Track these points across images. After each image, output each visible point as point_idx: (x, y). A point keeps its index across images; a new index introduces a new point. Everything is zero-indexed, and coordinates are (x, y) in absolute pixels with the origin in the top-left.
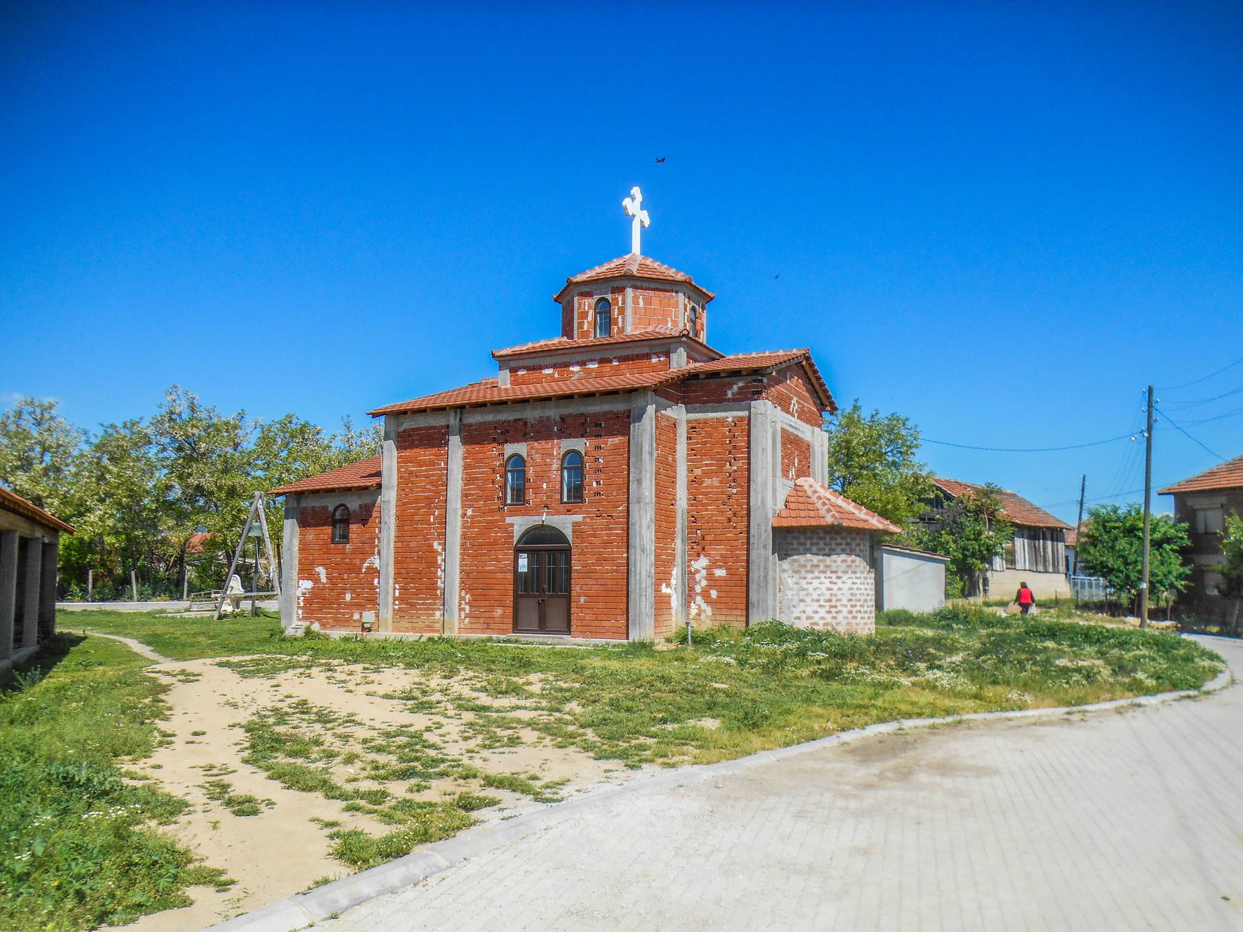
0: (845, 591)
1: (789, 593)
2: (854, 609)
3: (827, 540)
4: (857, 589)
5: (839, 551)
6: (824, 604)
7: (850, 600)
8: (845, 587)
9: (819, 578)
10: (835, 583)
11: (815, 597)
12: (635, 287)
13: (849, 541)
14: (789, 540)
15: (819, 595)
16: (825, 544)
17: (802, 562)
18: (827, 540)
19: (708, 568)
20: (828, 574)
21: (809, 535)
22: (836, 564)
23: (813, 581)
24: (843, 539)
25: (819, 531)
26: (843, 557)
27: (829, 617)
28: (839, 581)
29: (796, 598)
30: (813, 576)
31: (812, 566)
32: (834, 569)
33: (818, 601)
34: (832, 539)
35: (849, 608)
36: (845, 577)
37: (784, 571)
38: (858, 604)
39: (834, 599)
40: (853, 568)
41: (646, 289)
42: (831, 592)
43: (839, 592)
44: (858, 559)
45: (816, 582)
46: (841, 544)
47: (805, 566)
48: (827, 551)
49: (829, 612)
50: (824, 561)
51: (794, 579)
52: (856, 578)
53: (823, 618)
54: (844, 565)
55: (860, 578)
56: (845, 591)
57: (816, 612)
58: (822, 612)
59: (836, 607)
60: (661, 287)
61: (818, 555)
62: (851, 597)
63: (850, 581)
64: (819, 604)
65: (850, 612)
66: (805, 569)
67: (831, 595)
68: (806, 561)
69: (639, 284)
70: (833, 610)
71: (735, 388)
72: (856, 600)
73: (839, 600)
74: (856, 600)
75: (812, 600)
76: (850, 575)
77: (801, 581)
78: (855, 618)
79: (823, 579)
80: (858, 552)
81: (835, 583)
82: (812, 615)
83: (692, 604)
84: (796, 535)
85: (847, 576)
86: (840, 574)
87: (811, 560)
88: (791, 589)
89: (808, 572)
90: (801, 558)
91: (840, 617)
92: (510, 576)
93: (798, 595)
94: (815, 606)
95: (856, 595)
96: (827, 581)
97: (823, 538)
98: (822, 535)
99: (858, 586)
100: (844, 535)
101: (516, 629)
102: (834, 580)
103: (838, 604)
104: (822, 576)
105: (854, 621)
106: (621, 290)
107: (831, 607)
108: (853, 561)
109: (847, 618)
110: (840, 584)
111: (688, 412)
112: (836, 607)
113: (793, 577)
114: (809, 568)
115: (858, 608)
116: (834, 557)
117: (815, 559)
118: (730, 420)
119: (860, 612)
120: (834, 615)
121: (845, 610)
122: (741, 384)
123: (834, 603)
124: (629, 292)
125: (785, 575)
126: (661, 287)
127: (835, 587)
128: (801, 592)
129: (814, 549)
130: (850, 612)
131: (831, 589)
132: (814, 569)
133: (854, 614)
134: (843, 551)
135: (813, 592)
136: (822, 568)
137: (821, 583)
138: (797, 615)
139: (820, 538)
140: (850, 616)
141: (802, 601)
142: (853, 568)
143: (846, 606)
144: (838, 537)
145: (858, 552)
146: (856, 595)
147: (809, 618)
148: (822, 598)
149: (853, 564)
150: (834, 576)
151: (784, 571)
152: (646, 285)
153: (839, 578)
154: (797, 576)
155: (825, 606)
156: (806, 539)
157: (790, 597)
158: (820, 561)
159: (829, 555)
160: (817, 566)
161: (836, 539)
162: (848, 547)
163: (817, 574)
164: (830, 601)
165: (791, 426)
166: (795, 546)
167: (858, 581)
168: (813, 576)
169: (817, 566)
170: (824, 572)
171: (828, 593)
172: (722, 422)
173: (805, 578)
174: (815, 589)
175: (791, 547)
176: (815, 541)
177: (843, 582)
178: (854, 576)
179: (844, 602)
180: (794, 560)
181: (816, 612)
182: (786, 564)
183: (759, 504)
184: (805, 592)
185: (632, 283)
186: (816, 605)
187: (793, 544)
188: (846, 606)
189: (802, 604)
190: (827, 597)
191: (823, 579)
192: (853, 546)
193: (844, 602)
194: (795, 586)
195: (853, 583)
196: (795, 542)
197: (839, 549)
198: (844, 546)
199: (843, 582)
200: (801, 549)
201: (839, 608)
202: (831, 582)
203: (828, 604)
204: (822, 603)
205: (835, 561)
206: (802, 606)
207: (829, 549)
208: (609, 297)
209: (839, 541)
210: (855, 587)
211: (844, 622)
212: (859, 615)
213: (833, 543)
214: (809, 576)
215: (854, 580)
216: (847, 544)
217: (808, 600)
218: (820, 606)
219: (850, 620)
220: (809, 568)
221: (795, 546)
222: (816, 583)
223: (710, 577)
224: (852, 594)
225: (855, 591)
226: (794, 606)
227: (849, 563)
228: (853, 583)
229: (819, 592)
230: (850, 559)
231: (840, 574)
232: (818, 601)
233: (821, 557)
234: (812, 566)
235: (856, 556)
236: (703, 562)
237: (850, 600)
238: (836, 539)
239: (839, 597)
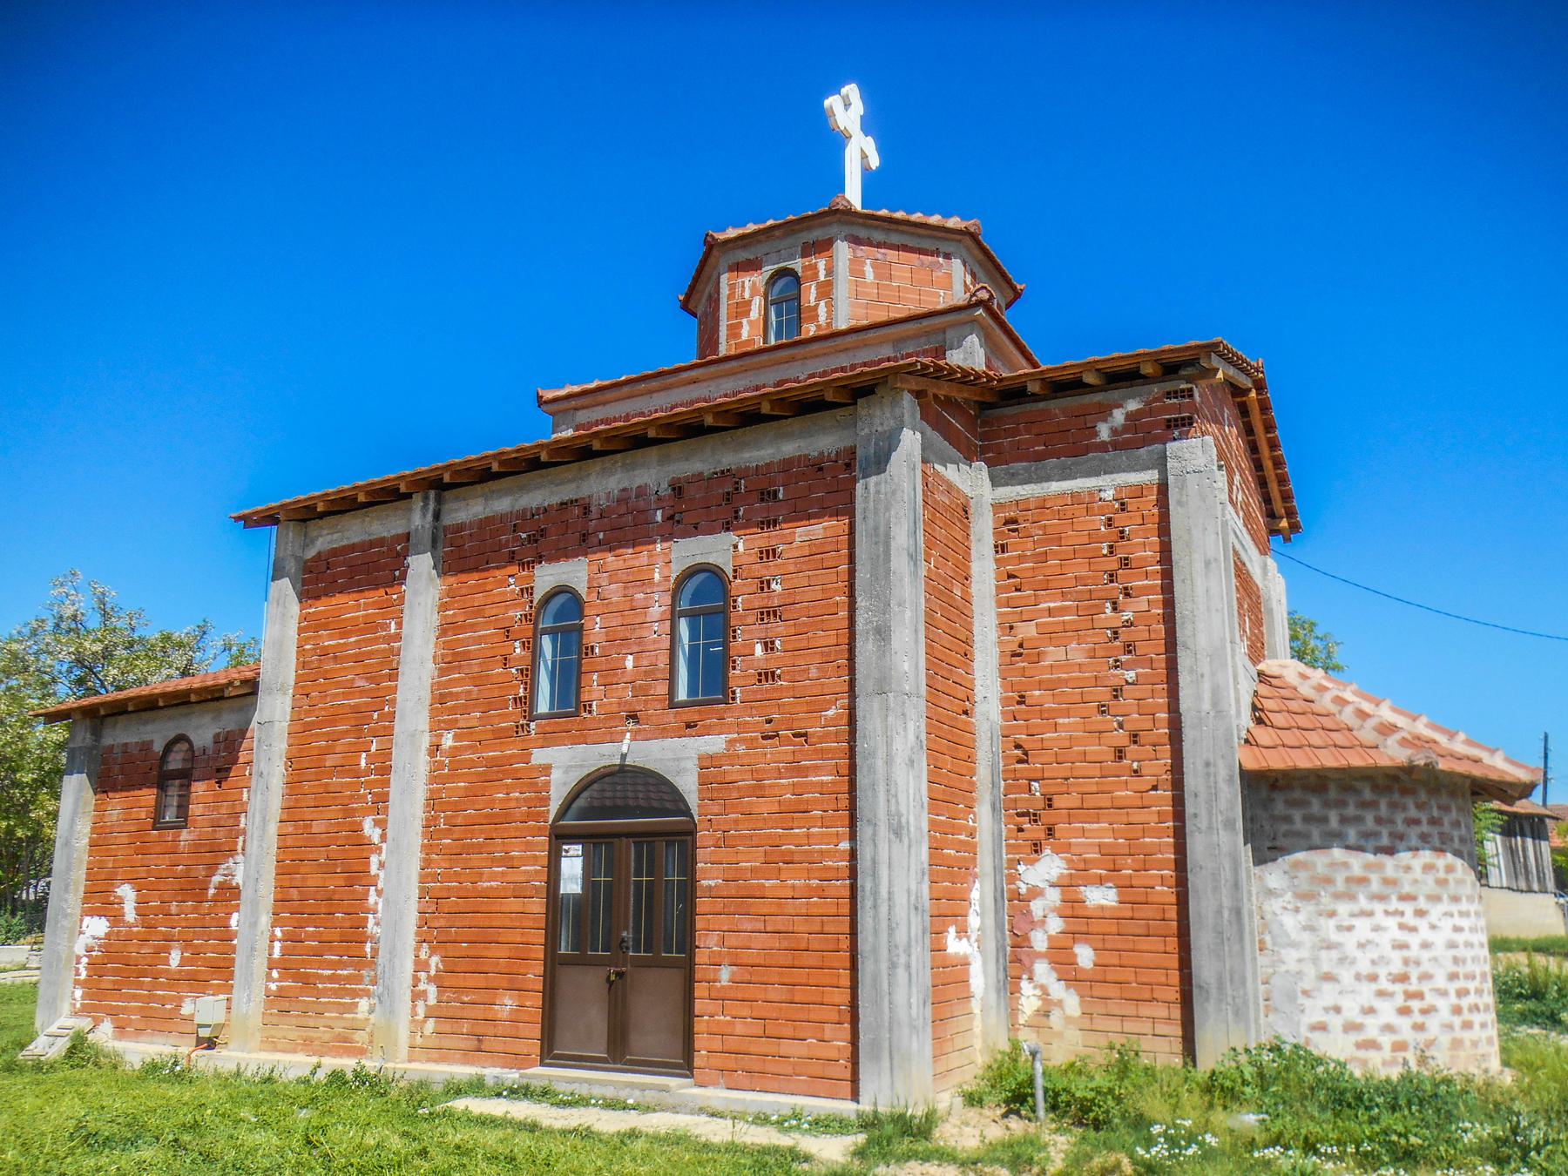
0: (1440, 950)
1: (1290, 956)
2: (1465, 1002)
3: (1384, 810)
6: (1390, 987)
7: (1453, 977)
8: (1439, 938)
9: (1370, 914)
10: (1413, 929)
11: (1364, 967)
12: (856, 241)
13: (1435, 813)
14: (1280, 808)
15: (1373, 962)
16: (1379, 821)
17: (1321, 869)
18: (1384, 810)
19: (1066, 885)
20: (1394, 904)
21: (1333, 794)
23: (1356, 922)
24: (1420, 806)
25: (1358, 785)
26: (1426, 856)
27: (1404, 1023)
28: (1422, 924)
29: (1310, 971)
30: (1355, 908)
31: (1349, 880)
32: (1407, 889)
33: (1373, 978)
34: (1393, 806)
35: (1453, 999)
36: (1436, 911)
37: (1271, 893)
39: (1414, 974)
41: (879, 246)
42: (1405, 953)
43: (1425, 955)
45: (1362, 925)
46: (1417, 822)
47: (1328, 881)
48: (1385, 841)
49: (1404, 1011)
50: (1380, 867)
51: (1302, 917)
52: (1461, 914)
53: (1388, 1028)
54: (1430, 879)
56: (1440, 950)
57: (1370, 1011)
58: (1387, 1011)
59: (1419, 995)
60: (911, 243)
61: (1361, 849)
62: (1454, 969)
64: (1374, 987)
66: (1331, 889)
67: (1406, 962)
68: (1332, 865)
70: (1415, 1005)
71: (1119, 416)
73: (1426, 977)
75: (1358, 977)
76: (1444, 906)
77: (1323, 921)
78: (1467, 1025)
79: (1380, 918)
81: (1413, 929)
82: (1359, 1019)
83: (1025, 985)
84: (1297, 794)
86: (1422, 903)
87: (1346, 865)
88: (1295, 945)
89: (1338, 896)
90: (1319, 860)
91: (1433, 1024)
92: (538, 906)
93: (1315, 961)
94: (1366, 992)
96: (1392, 923)
97: (1372, 805)
98: (1368, 795)
101: (550, 1052)
102: (1410, 919)
103: (1425, 987)
104: (1378, 907)
106: (824, 246)
107: (1409, 995)
109: (1450, 1027)
110: (1425, 933)
111: (995, 482)
112: (1419, 995)
113: (1297, 910)
114: (1340, 885)
116: (1404, 857)
117: (1358, 862)
118: (1109, 495)
120: (1417, 1018)
121: (1444, 1005)
122: (1133, 405)
123: (1414, 986)
124: (843, 250)
125: (1274, 905)
126: (911, 243)
127: (1414, 940)
128: (1324, 954)
129: (1352, 834)
131: (1403, 946)
132: (1355, 888)
133: (1466, 1016)
134: (1424, 838)
135: (1358, 954)
136: (1375, 886)
137: (1376, 929)
138: (1319, 1017)
139: (1364, 805)
140: (1457, 1021)
141: (1328, 977)
143: (1444, 993)
144: (1410, 802)
146: (1464, 961)
147: (1351, 1027)
148: (1382, 972)
149: (1450, 877)
150: (1408, 908)
151: (1271, 893)
152: (878, 236)
153: (1420, 913)
154: (1308, 909)
155: (1391, 995)
156: (1327, 805)
157: (1292, 966)
158: (1368, 867)
159: (1390, 851)
160: (1363, 881)
161: (1404, 808)
162: (1435, 831)
163: (1363, 903)
164: (1403, 978)
166: (1299, 825)
168: (1355, 908)
169: (1363, 881)
170: (1381, 898)
171: (1396, 957)
172: (1087, 502)
173: (1332, 914)
174: (1361, 946)
175: (1284, 827)
176: (1351, 811)
178: (1454, 908)
179: (1440, 981)
180: (1297, 865)
181: (1370, 1011)
182: (1274, 875)
183: (1206, 706)
184: (1334, 954)
185: (846, 230)
186: (1367, 989)
187: (1288, 819)
188: (1444, 993)
189: (1327, 987)
190: (1397, 967)
191: (1380, 918)
192: (1447, 827)
193: (1440, 981)
194: (1306, 937)
196: (1297, 815)
197: (1413, 834)
198: (1425, 828)
200: (1316, 834)
201: (1430, 999)
202: (1402, 927)
203: (1398, 988)
204: (1384, 984)
205: (1408, 869)
206: (1328, 996)
207: (1391, 834)
208: (797, 264)
209: (1413, 812)
210: (1460, 938)
213: (1399, 818)
214: (1343, 908)
216: (1433, 822)
217: (1346, 976)
218: (1381, 994)
219: (1458, 1033)
220: (1340, 885)
221: (1299, 825)
222: (1363, 927)
223: (1072, 908)
224: (1456, 960)
226: (1306, 993)
227: (1442, 875)
229: (1372, 954)
231: (1422, 903)
232: (1373, 978)
233: (1370, 857)
234: (1349, 880)
236: (1048, 868)
237: (1453, 977)
238: (1404, 808)
239: (1426, 967)
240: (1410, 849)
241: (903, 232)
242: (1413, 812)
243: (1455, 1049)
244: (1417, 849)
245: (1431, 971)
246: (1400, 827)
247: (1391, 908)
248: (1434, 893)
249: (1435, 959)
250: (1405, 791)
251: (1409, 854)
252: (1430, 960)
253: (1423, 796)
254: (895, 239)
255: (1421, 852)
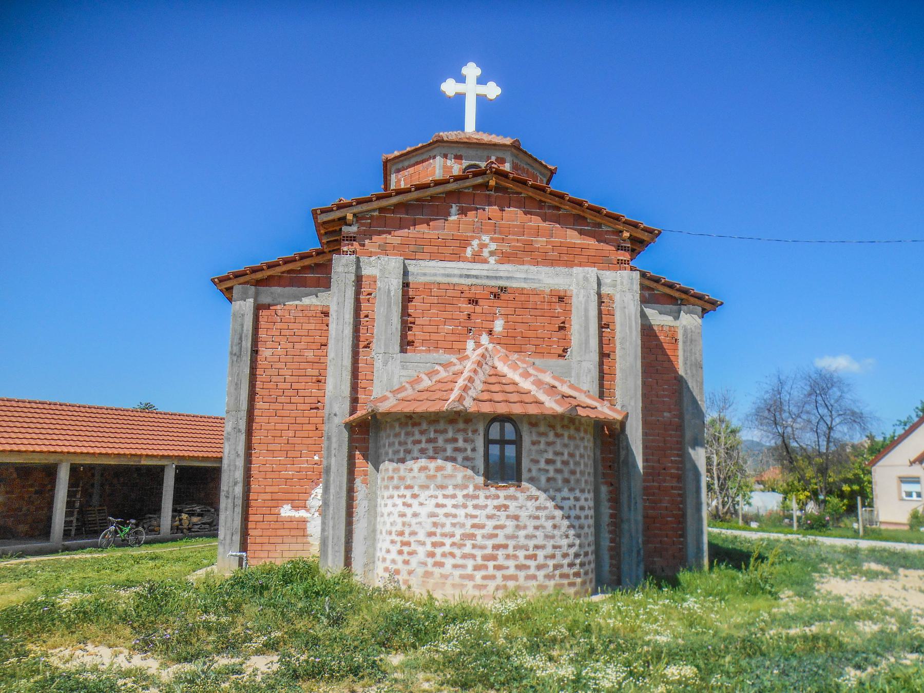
0: (423, 518)
2: (439, 551)
4: (447, 515)
5: (416, 453)
7: (431, 534)
8: (424, 511)
10: (410, 506)
13: (432, 435)
16: (400, 444)
20: (402, 491)
22: (411, 475)
24: (422, 433)
26: (423, 462)
28: (415, 502)
32: (409, 482)
34: (407, 434)
35: (429, 548)
36: (424, 495)
38: (448, 541)
40: (439, 480)
42: (404, 519)
43: (414, 521)
44: (449, 465)
48: (402, 455)
52: (445, 496)
54: (423, 475)
55: (454, 496)
56: (423, 518)
59: (408, 544)
60: (419, 159)
62: (433, 530)
63: (434, 501)
65: (432, 555)
67: (404, 524)
69: (400, 166)
70: (406, 549)
72: (444, 535)
73: (413, 533)
74: (444, 535)
76: (431, 492)
78: (440, 565)
80: (449, 453)
81: (410, 506)
85: (428, 493)
86: (416, 490)
91: (414, 561)
95: (443, 525)
99: (449, 510)
100: (424, 426)
102: (409, 500)
103: (412, 539)
105: (437, 571)
107: (404, 544)
108: (439, 469)
109: (425, 564)
110: (416, 508)
112: (408, 544)
115: (447, 549)
116: (410, 464)
119: (453, 555)
120: (406, 557)
121: (421, 551)
123: (406, 538)
126: (419, 159)
127: (409, 511)
130: (432, 555)
131: (403, 515)
133: (438, 558)
134: (423, 451)
140: (430, 561)
142: (439, 480)
143: (424, 544)
144: (416, 430)
145: (449, 453)
146: (443, 525)
149: (439, 474)
150: (408, 493)
153: (415, 496)
159: (403, 461)
162: (430, 446)
165: (468, 276)
167: (449, 502)
171: (400, 520)
177: (421, 504)
178: (440, 493)
179: (421, 536)
190: (399, 527)
192: (440, 442)
195: (438, 505)
197: (416, 448)
198: (423, 445)
199: (421, 504)
201: (414, 546)
202: (404, 504)
203: (399, 539)
207: (405, 451)
209: (417, 437)
210: (441, 511)
211: (420, 571)
212: (449, 562)
215: (441, 500)
216: (429, 441)
219: (430, 568)
224: (435, 524)
225: (442, 519)
227: (432, 473)
228: (438, 505)
230: (432, 465)
231: (416, 490)
233: (395, 464)
235: (447, 459)
237: (431, 534)
239: (414, 528)
240: (413, 459)
241: (413, 156)
242: (417, 437)
243: (427, 578)
244: (418, 458)
245: (416, 530)
246: (410, 446)
247: (401, 494)
248: (424, 484)
249: (420, 523)
250: (415, 424)
251: (413, 462)
252: (416, 524)
253: (424, 426)
254: (413, 161)
255: (419, 460)
